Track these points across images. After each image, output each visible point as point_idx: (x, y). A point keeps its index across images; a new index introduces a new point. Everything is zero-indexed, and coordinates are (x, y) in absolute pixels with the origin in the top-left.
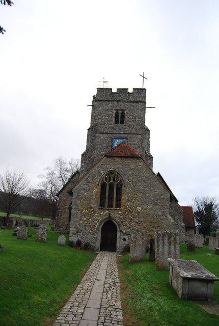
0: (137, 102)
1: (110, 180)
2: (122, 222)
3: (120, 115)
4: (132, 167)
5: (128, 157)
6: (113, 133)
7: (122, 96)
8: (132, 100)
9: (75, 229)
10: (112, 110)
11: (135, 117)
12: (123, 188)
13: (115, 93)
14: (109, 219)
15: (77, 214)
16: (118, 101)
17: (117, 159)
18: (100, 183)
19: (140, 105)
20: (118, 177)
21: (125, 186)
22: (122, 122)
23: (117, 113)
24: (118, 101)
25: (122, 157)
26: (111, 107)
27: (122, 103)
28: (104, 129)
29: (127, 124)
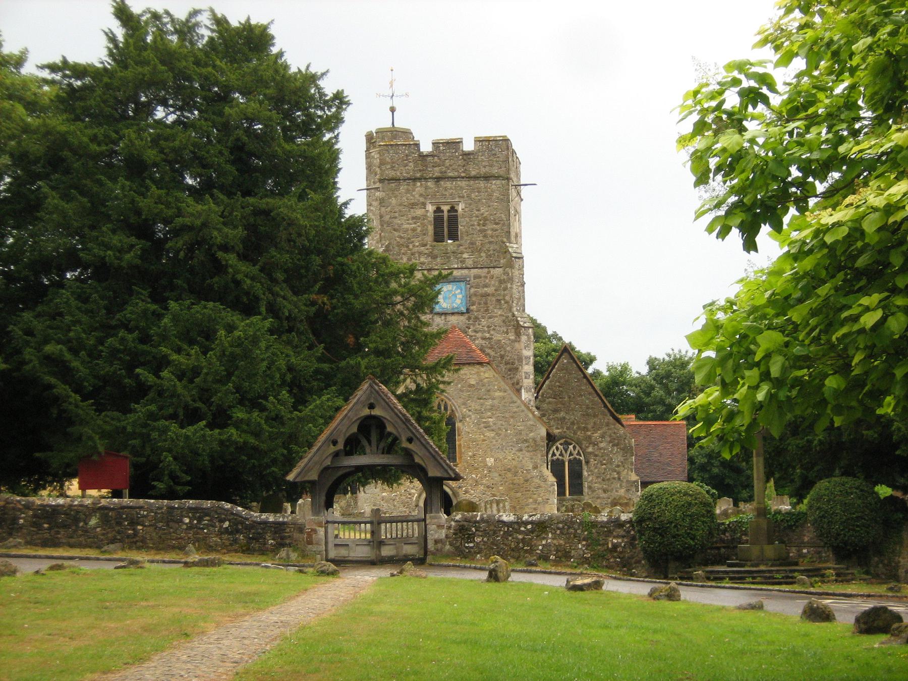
0: (487, 178)
3: (446, 214)
7: (447, 163)
8: (473, 173)
10: (424, 204)
11: (485, 219)
16: (438, 179)
19: (495, 184)
21: (461, 421)
22: (454, 236)
23: (438, 210)
24: (438, 179)
26: (421, 195)
27: (448, 184)
29: (465, 240)
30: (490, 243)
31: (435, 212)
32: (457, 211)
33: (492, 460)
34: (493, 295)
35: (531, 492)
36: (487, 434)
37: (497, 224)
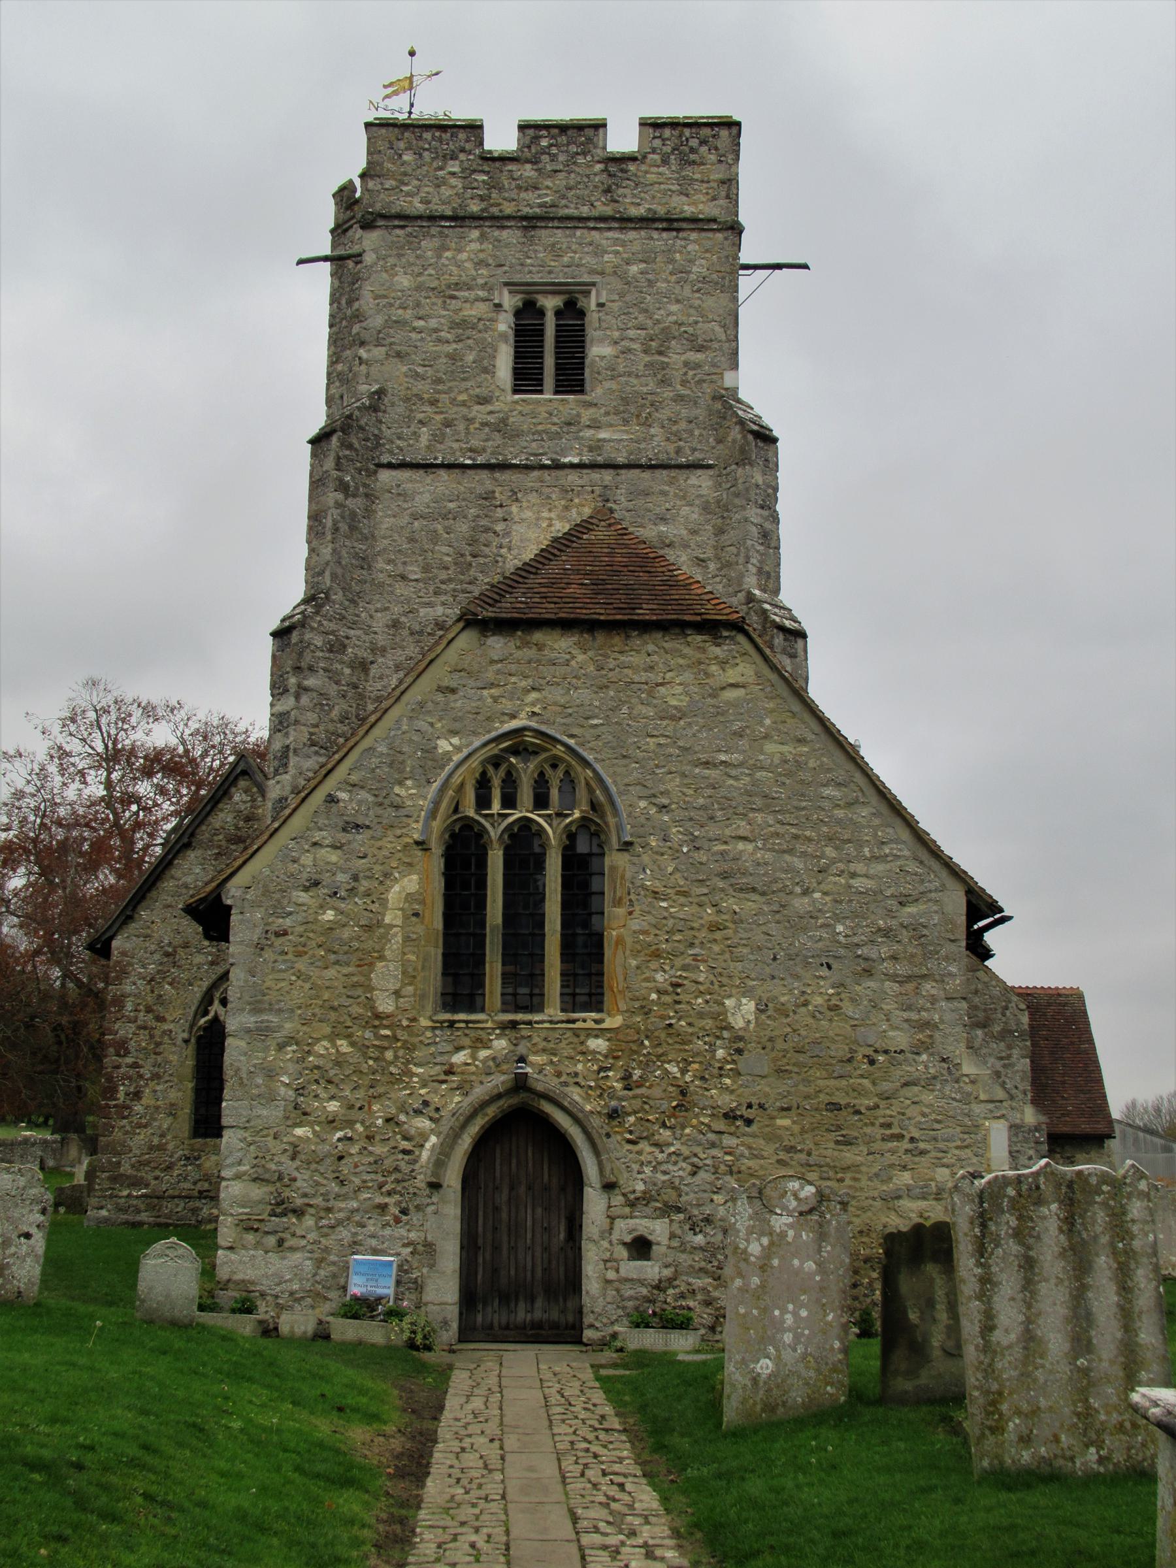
0: (672, 223)
1: (509, 801)
2: (614, 1115)
4: (674, 696)
5: (645, 627)
6: (504, 466)
9: (258, 1192)
12: (615, 860)
13: (504, 159)
14: (514, 1101)
15: (271, 1074)
17: (561, 644)
18: (437, 825)
19: (693, 243)
20: (569, 780)
21: (627, 846)
23: (528, 312)
25: (590, 626)
28: (438, 438)
30: (680, 398)
31: (518, 314)
32: (581, 314)
33: (749, 1006)
34: (686, 546)
35: (905, 1145)
36: (730, 903)
37: (700, 349)
